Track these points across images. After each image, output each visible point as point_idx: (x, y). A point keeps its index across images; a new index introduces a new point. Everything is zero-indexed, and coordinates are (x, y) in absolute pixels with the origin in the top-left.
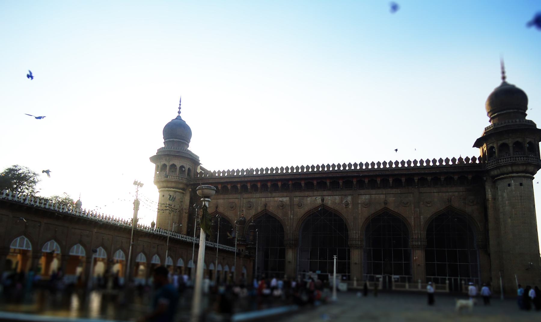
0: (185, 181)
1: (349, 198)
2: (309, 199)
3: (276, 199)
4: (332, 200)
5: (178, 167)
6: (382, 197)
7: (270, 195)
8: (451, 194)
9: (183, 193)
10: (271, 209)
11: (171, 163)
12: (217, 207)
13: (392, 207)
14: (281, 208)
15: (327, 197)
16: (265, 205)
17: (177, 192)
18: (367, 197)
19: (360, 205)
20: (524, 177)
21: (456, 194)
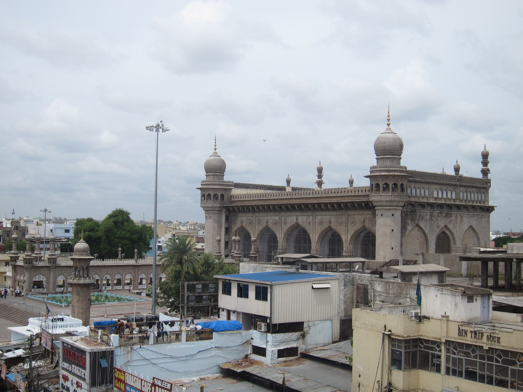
0: (218, 205)
1: (311, 218)
2: (290, 218)
4: (303, 219)
5: (212, 196)
8: (365, 216)
10: (270, 225)
11: (208, 193)
12: (242, 223)
13: (333, 226)
18: (319, 217)
20: (384, 209)
21: (368, 216)
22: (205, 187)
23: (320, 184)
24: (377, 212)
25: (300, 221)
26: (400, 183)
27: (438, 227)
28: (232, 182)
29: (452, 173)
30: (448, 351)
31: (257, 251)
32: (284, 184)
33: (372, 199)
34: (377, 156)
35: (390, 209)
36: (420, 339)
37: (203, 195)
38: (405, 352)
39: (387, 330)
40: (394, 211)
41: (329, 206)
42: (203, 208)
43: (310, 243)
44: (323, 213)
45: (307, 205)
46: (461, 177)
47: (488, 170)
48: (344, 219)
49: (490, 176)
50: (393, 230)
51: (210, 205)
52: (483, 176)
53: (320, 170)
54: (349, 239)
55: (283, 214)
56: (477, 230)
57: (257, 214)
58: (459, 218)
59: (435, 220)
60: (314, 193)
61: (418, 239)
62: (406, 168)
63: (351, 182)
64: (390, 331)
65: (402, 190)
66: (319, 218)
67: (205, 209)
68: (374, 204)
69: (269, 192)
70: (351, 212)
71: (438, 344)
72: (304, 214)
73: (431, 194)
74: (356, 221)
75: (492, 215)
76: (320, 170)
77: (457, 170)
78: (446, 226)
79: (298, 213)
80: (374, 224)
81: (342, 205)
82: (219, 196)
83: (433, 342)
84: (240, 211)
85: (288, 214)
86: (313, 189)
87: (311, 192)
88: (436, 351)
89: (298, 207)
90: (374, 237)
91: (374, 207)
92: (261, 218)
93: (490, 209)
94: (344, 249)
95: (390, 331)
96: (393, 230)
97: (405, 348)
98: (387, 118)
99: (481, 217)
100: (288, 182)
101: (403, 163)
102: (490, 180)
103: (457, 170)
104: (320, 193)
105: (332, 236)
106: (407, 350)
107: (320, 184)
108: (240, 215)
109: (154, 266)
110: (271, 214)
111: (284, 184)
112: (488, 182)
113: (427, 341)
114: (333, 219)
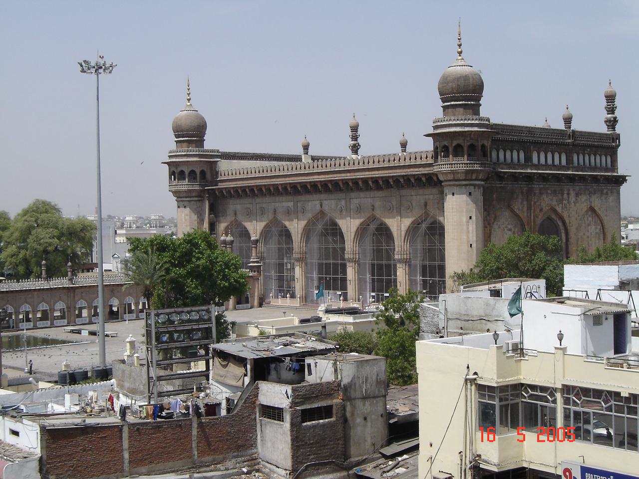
1: (343, 202)
2: (310, 204)
3: (284, 203)
4: (330, 204)
5: (187, 173)
6: (370, 201)
7: (277, 198)
8: (427, 196)
9: (201, 200)
11: (179, 169)
12: (235, 214)
14: (287, 215)
15: (325, 201)
16: (275, 211)
17: (191, 201)
19: (352, 211)
21: (431, 197)
22: (174, 160)
23: (355, 149)
24: (446, 190)
25: (326, 208)
26: (480, 144)
27: (541, 210)
28: (218, 151)
29: (561, 126)
30: (567, 401)
31: (262, 258)
32: (299, 151)
33: (436, 169)
34: (444, 102)
35: (466, 185)
36: (522, 385)
37: (172, 173)
38: (501, 407)
39: (472, 371)
40: (472, 187)
41: (370, 183)
42: (175, 193)
43: (343, 240)
44: (362, 194)
45: (335, 183)
46: (573, 132)
47: (615, 118)
48: (394, 203)
49: (618, 129)
50: (470, 218)
51: (185, 188)
52: (608, 129)
53: (355, 129)
54: (403, 233)
55: (300, 198)
56: (599, 212)
57: (258, 200)
58: (572, 193)
59: (536, 200)
60: (347, 164)
61: (510, 230)
62: (488, 120)
63: (404, 145)
64: (475, 373)
65: (485, 155)
66: (355, 202)
67: (178, 195)
68: (441, 178)
69: (276, 163)
70: (404, 192)
71: (552, 391)
72: (333, 196)
73: (528, 159)
74: (414, 204)
75: (623, 188)
76: (355, 129)
77: (568, 120)
78: (554, 210)
79: (323, 196)
80: (442, 209)
81: (391, 181)
82: (198, 173)
83: (543, 389)
84: (231, 196)
85: (308, 197)
86: (345, 158)
87: (342, 162)
88: (547, 401)
89: (322, 186)
90: (442, 228)
91: (441, 182)
92: (264, 205)
93: (622, 180)
94: (397, 250)
95: (475, 373)
96: (470, 218)
97: (501, 400)
98: (458, 42)
99: (607, 194)
100: (306, 148)
101: (484, 112)
102: (619, 135)
103: (568, 120)
104: (356, 163)
105: (377, 229)
106: (504, 403)
107: (355, 149)
108: (231, 201)
109: (100, 289)
110: (281, 198)
111: (299, 151)
112: (616, 138)
113: (533, 387)
114: (378, 204)
